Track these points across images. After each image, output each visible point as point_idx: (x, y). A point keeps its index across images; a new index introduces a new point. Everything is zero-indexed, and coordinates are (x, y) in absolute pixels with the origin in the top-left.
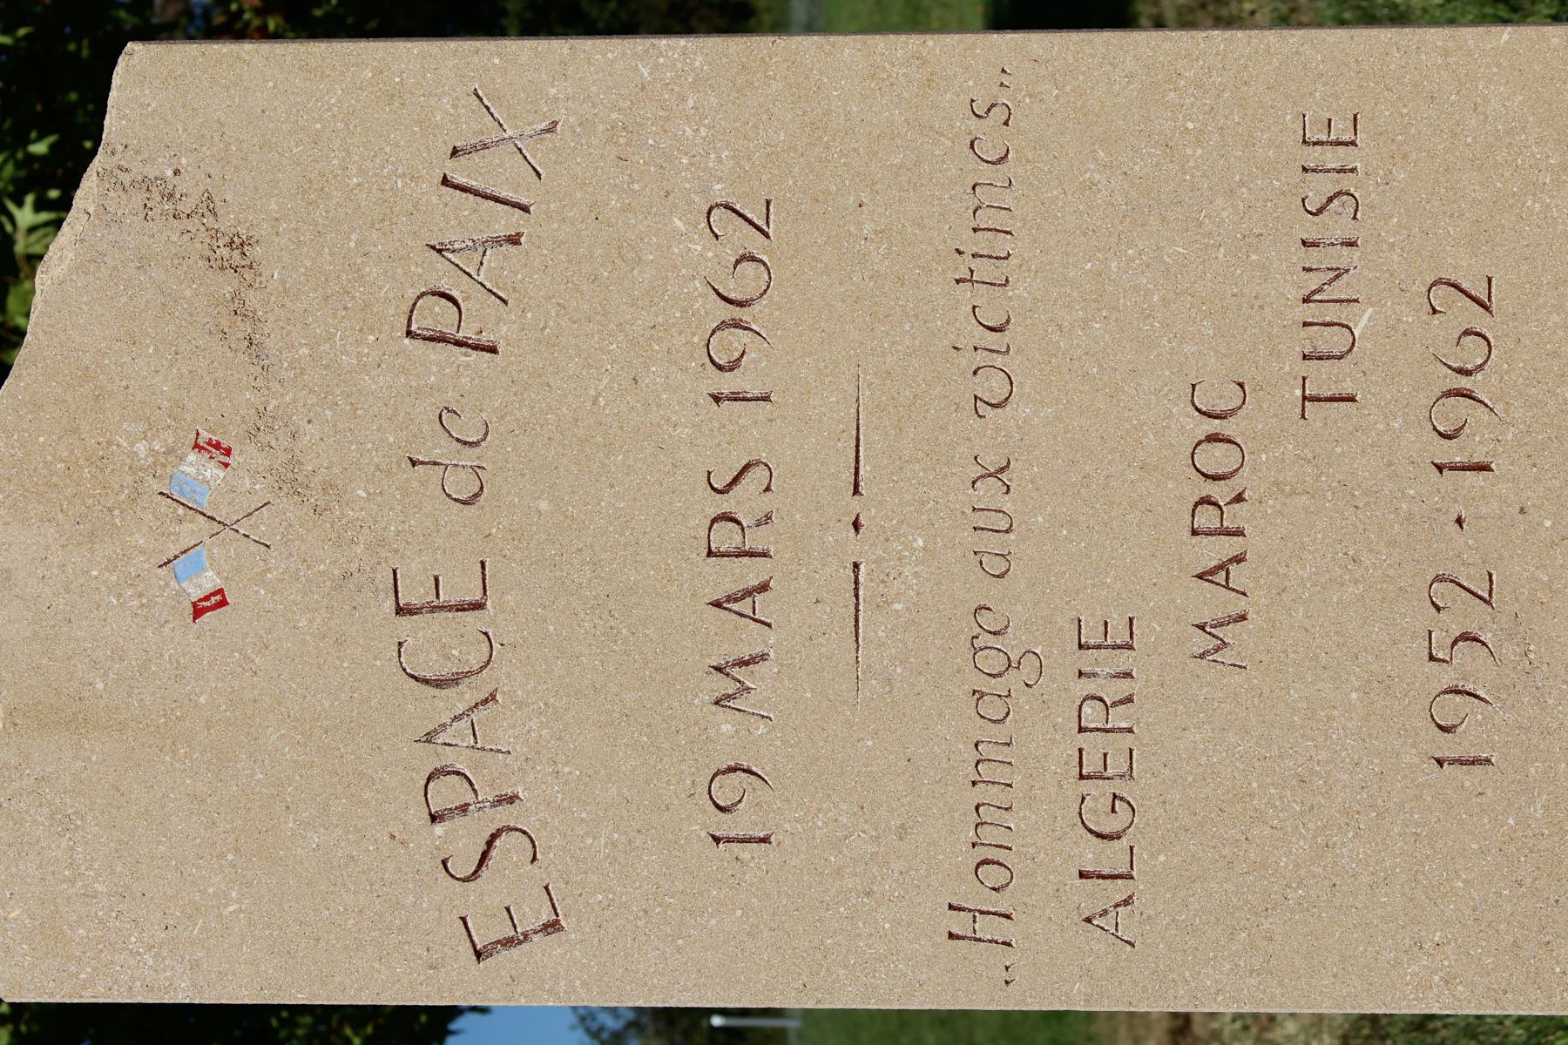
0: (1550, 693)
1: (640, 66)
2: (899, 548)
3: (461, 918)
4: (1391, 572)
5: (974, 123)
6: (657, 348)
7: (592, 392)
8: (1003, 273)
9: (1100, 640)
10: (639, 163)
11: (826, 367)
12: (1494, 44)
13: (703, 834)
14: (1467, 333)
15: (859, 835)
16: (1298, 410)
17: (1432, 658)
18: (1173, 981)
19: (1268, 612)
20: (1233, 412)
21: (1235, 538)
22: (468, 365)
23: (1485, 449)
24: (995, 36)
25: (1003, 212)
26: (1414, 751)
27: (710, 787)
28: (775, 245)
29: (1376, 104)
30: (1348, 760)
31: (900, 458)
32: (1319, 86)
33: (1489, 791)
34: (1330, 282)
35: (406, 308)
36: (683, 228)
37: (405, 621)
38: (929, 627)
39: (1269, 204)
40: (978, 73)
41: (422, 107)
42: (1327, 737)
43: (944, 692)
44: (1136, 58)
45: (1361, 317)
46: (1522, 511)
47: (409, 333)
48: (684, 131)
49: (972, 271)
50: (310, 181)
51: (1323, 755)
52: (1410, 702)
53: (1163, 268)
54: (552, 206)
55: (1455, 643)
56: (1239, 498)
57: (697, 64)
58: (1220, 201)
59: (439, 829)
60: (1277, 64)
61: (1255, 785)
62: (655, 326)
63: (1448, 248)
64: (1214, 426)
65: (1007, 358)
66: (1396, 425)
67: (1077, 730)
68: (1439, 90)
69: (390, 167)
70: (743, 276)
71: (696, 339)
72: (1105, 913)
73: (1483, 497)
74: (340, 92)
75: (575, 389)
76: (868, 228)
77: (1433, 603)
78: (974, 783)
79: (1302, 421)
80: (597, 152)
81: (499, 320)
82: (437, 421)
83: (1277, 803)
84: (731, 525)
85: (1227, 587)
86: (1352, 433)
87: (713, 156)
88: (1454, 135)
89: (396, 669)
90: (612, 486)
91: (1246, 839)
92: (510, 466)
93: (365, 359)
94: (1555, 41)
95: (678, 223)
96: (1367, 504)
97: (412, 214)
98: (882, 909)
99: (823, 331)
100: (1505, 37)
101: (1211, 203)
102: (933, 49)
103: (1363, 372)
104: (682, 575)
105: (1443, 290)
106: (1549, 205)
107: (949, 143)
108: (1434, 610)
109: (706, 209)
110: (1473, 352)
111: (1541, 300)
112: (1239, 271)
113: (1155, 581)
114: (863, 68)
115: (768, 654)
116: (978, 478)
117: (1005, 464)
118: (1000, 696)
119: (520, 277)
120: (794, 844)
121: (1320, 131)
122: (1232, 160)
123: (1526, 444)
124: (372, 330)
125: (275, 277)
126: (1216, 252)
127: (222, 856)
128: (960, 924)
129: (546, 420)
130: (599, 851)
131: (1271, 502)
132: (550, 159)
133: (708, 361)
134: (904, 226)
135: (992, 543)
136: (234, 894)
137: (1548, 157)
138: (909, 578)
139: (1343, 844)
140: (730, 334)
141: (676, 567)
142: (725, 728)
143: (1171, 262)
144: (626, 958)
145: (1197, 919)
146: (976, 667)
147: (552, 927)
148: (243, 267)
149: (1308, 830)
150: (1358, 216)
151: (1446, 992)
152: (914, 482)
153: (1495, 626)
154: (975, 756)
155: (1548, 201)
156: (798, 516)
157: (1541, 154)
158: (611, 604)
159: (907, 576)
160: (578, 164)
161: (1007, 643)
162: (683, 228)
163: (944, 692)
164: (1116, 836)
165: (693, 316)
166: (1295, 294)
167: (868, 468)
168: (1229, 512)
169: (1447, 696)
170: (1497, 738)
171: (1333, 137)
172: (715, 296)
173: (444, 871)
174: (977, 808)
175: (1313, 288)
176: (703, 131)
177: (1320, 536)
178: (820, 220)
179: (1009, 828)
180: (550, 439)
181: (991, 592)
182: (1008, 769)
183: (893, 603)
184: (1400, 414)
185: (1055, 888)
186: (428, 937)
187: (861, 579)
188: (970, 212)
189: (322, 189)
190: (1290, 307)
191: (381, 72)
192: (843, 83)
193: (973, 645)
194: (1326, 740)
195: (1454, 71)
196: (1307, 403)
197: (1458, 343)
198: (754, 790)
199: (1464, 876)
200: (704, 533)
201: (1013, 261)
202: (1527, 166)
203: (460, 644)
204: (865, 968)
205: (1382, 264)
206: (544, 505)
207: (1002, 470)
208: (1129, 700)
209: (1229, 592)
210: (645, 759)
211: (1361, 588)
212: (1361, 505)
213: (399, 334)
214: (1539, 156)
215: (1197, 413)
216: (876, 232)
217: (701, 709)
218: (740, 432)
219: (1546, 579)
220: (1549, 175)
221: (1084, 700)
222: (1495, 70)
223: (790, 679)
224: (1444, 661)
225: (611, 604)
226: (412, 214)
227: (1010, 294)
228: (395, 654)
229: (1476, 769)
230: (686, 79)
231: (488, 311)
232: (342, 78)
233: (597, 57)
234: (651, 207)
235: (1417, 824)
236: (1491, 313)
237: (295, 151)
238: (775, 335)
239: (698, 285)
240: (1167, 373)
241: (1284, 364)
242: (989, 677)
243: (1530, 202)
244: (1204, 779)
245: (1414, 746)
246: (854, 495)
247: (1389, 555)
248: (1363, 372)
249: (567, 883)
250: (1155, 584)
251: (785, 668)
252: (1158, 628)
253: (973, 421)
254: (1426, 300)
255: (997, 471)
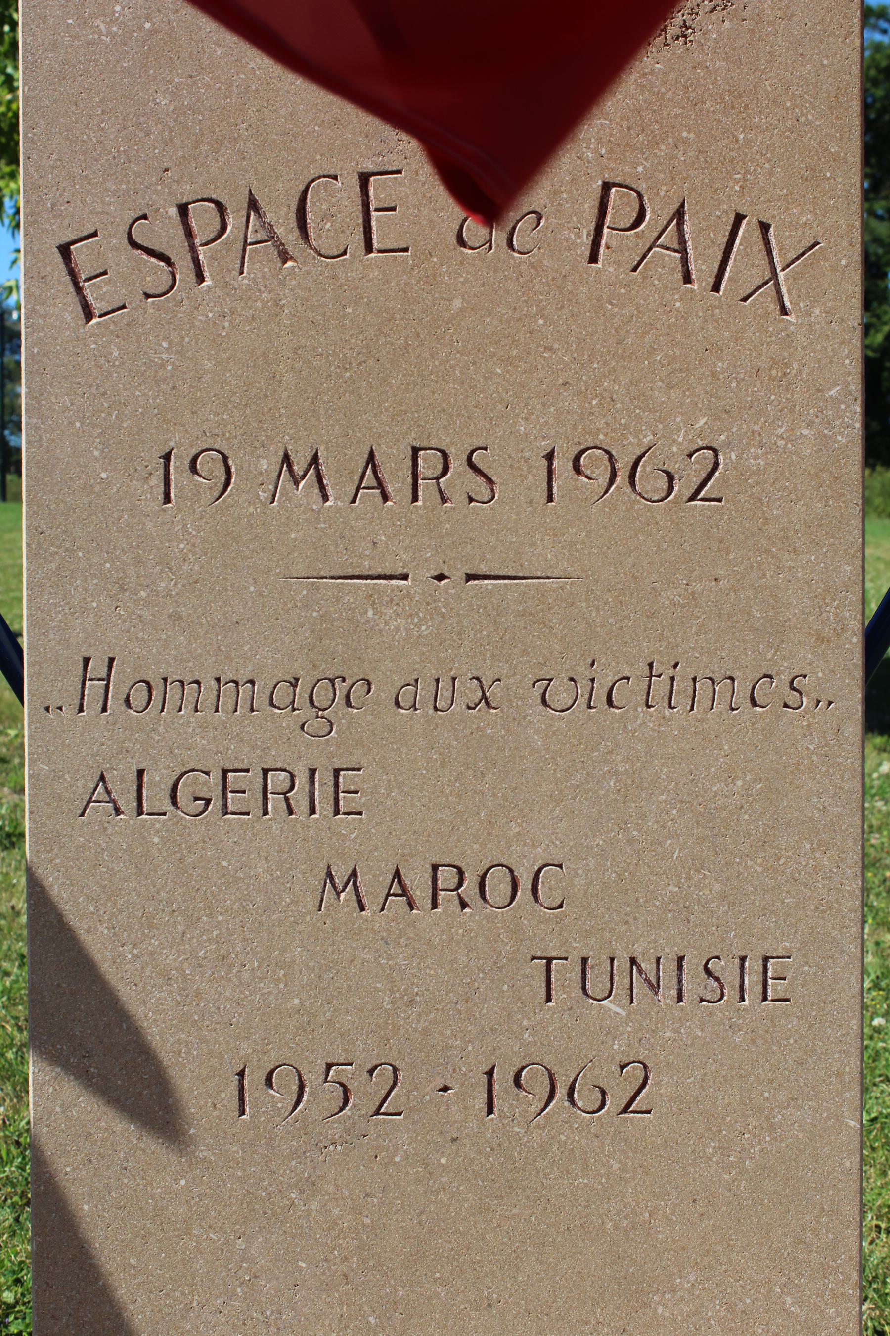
0: (300, 1163)
1: (838, 388)
2: (421, 615)
3: (96, 231)
4: (402, 1032)
5: (786, 678)
6: (594, 402)
7: (556, 346)
8: (657, 703)
9: (341, 787)
10: (754, 387)
11: (577, 551)
12: (846, 1114)
13: (172, 444)
14: (603, 1093)
15: (172, 580)
16: (539, 954)
17: (329, 1066)
18: (52, 850)
19: (367, 929)
20: (536, 898)
21: (430, 901)
22: (579, 237)
23: (506, 1109)
24: (860, 695)
25: (710, 703)
26: (250, 1051)
27: (213, 450)
28: (684, 506)
29: (797, 1017)
30: (242, 996)
31: (498, 615)
32: (814, 970)
33: (215, 1114)
34: (647, 980)
35: (628, 182)
36: (697, 426)
37: (355, 181)
38: (353, 640)
39: (714, 928)
40: (828, 681)
41: (805, 196)
42: (261, 979)
43: (296, 653)
44: (839, 816)
45: (618, 1005)
46: (454, 1140)
47: (607, 187)
48: (781, 427)
49: (659, 676)
50: (740, 97)
51: (246, 975)
52: (291, 1048)
53: (660, 839)
54: (718, 310)
55: (342, 1085)
56: (464, 905)
57: (839, 438)
58: (718, 887)
59: (173, 211)
60: (833, 935)
61: (220, 918)
62: (613, 401)
63: (675, 1078)
64: (525, 884)
65: (585, 706)
66: (526, 1036)
67: (265, 767)
68: (808, 1069)
69: (752, 168)
70: (656, 478)
71: (601, 437)
72: (108, 792)
73: (465, 1108)
74: (818, 123)
75: (558, 331)
76: (698, 587)
77: (376, 1067)
78: (218, 680)
79: (529, 957)
80: (765, 351)
81: (618, 263)
82: (531, 209)
83: (204, 937)
84: (440, 467)
85: (388, 895)
86: (520, 998)
87: (760, 451)
88: (771, 1081)
89: (314, 173)
90: (474, 363)
91: (174, 911)
92: (491, 273)
93: (585, 145)
94: (848, 1164)
95: (702, 421)
96: (460, 1012)
97: (711, 187)
98: (108, 600)
99: (608, 548)
100: (852, 1123)
101: (716, 880)
102: (851, 643)
103: (571, 1008)
104: (396, 425)
105: (640, 1074)
106: (710, 1159)
107: (769, 656)
108: (369, 1067)
109: (715, 445)
110: (586, 1098)
111: (631, 1154)
112: (657, 903)
113: (394, 833)
114: (834, 582)
115: (328, 500)
116: (480, 682)
117: (493, 705)
118: (294, 701)
119: (656, 282)
120: (163, 523)
121: (775, 971)
122: (752, 898)
123: (510, 1143)
124: (611, 151)
125: (657, 66)
126: (674, 884)
127: (148, 18)
128: (97, 668)
129: (532, 305)
130: (156, 353)
131: (461, 931)
132: (759, 309)
133: (583, 447)
134: (699, 617)
135: (424, 691)
136: (115, 29)
137: (751, 1158)
138: (395, 623)
139: (171, 992)
140: (606, 467)
141: (403, 420)
142: (264, 464)
143: (666, 846)
144: (64, 377)
145: (105, 870)
146: (319, 681)
147: (89, 315)
148: (666, 38)
149: (182, 963)
150: (704, 1003)
151: (47, 1078)
152: (478, 627)
153: (356, 1118)
154: (242, 680)
155: (714, 1159)
156: (448, 526)
157: (754, 1153)
158: (371, 363)
159: (396, 621)
160: (754, 333)
161: (338, 710)
162: (697, 426)
163: (296, 653)
164: (174, 802)
165: (622, 434)
166: (638, 950)
167: (490, 587)
168: (452, 895)
169: (297, 1078)
170: (262, 1119)
171: (770, 981)
172: (639, 453)
173: (137, 216)
174: (198, 683)
175: (643, 965)
176: (781, 443)
177: (432, 972)
178: (705, 545)
179: (180, 710)
180: (515, 309)
181: (382, 692)
182: (231, 707)
183: (373, 609)
184: (536, 1038)
185: (129, 749)
186: (79, 202)
187: (394, 582)
188: (710, 675)
189: (733, 107)
190: (627, 947)
191: (834, 160)
192: (822, 565)
193: (338, 678)
194: (259, 978)
195: (824, 1080)
196: (545, 961)
197: (596, 1087)
198: (211, 488)
199: (145, 1092)
200: (433, 443)
201: (667, 712)
202: (743, 1142)
203: (335, 230)
204: (58, 585)
205: (663, 1023)
206: (457, 303)
207: (488, 704)
208: (291, 812)
209: (384, 896)
210: (236, 393)
211: (389, 1007)
212: (459, 1007)
213: (606, 176)
214: (752, 1151)
215: (536, 868)
216: (693, 593)
217: (280, 442)
218: (521, 476)
219: (397, 1159)
220: (736, 1160)
221: (290, 773)
222: (825, 1115)
223: (306, 519)
224: (327, 1076)
225: (371, 363)
226: (711, 187)
227: (640, 709)
228: (326, 173)
229: (235, 1103)
230: (826, 428)
231: (627, 254)
232: (830, 125)
233: (846, 350)
234: (716, 398)
235: (188, 1053)
236: (621, 1113)
237: (767, 83)
238: (605, 506)
239: (648, 439)
240: (571, 844)
241: (579, 942)
242: (309, 691)
243: (713, 1144)
244: (224, 876)
245: (254, 1051)
246: (467, 574)
247: (416, 1030)
248: (571, 1008)
249: (128, 325)
250: (390, 833)
251: (316, 515)
252: (353, 836)
253: (531, 678)
254: (632, 1060)
255: (486, 699)
